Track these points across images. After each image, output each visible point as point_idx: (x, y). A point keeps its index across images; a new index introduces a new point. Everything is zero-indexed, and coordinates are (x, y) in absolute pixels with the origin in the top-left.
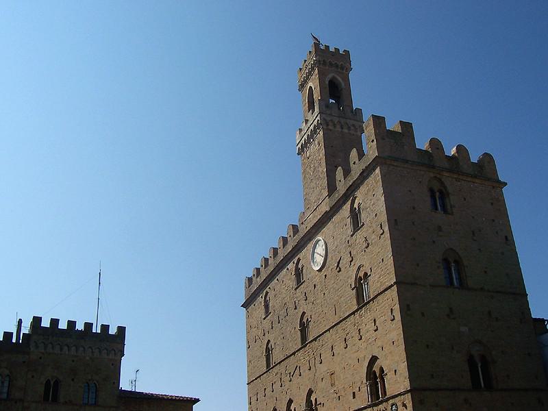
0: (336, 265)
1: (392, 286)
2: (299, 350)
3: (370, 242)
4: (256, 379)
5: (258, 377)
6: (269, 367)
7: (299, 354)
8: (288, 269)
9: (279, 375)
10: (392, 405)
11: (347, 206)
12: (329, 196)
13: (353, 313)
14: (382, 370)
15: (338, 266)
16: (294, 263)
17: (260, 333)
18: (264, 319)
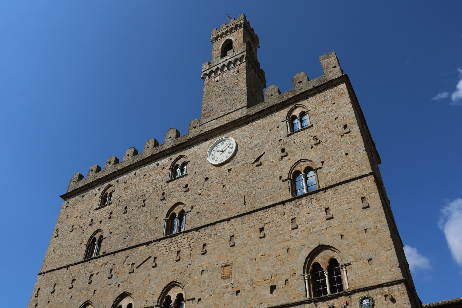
0: (253, 161)
1: (366, 175)
2: (159, 240)
3: (323, 140)
4: (59, 269)
5: (64, 267)
6: (88, 257)
7: (158, 244)
8: (158, 165)
9: (109, 266)
10: (365, 298)
11: (285, 112)
12: (248, 106)
13: (283, 203)
14: (333, 263)
15: (258, 159)
16: (171, 159)
17: (85, 222)
18: (97, 209)
